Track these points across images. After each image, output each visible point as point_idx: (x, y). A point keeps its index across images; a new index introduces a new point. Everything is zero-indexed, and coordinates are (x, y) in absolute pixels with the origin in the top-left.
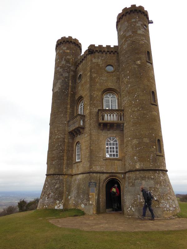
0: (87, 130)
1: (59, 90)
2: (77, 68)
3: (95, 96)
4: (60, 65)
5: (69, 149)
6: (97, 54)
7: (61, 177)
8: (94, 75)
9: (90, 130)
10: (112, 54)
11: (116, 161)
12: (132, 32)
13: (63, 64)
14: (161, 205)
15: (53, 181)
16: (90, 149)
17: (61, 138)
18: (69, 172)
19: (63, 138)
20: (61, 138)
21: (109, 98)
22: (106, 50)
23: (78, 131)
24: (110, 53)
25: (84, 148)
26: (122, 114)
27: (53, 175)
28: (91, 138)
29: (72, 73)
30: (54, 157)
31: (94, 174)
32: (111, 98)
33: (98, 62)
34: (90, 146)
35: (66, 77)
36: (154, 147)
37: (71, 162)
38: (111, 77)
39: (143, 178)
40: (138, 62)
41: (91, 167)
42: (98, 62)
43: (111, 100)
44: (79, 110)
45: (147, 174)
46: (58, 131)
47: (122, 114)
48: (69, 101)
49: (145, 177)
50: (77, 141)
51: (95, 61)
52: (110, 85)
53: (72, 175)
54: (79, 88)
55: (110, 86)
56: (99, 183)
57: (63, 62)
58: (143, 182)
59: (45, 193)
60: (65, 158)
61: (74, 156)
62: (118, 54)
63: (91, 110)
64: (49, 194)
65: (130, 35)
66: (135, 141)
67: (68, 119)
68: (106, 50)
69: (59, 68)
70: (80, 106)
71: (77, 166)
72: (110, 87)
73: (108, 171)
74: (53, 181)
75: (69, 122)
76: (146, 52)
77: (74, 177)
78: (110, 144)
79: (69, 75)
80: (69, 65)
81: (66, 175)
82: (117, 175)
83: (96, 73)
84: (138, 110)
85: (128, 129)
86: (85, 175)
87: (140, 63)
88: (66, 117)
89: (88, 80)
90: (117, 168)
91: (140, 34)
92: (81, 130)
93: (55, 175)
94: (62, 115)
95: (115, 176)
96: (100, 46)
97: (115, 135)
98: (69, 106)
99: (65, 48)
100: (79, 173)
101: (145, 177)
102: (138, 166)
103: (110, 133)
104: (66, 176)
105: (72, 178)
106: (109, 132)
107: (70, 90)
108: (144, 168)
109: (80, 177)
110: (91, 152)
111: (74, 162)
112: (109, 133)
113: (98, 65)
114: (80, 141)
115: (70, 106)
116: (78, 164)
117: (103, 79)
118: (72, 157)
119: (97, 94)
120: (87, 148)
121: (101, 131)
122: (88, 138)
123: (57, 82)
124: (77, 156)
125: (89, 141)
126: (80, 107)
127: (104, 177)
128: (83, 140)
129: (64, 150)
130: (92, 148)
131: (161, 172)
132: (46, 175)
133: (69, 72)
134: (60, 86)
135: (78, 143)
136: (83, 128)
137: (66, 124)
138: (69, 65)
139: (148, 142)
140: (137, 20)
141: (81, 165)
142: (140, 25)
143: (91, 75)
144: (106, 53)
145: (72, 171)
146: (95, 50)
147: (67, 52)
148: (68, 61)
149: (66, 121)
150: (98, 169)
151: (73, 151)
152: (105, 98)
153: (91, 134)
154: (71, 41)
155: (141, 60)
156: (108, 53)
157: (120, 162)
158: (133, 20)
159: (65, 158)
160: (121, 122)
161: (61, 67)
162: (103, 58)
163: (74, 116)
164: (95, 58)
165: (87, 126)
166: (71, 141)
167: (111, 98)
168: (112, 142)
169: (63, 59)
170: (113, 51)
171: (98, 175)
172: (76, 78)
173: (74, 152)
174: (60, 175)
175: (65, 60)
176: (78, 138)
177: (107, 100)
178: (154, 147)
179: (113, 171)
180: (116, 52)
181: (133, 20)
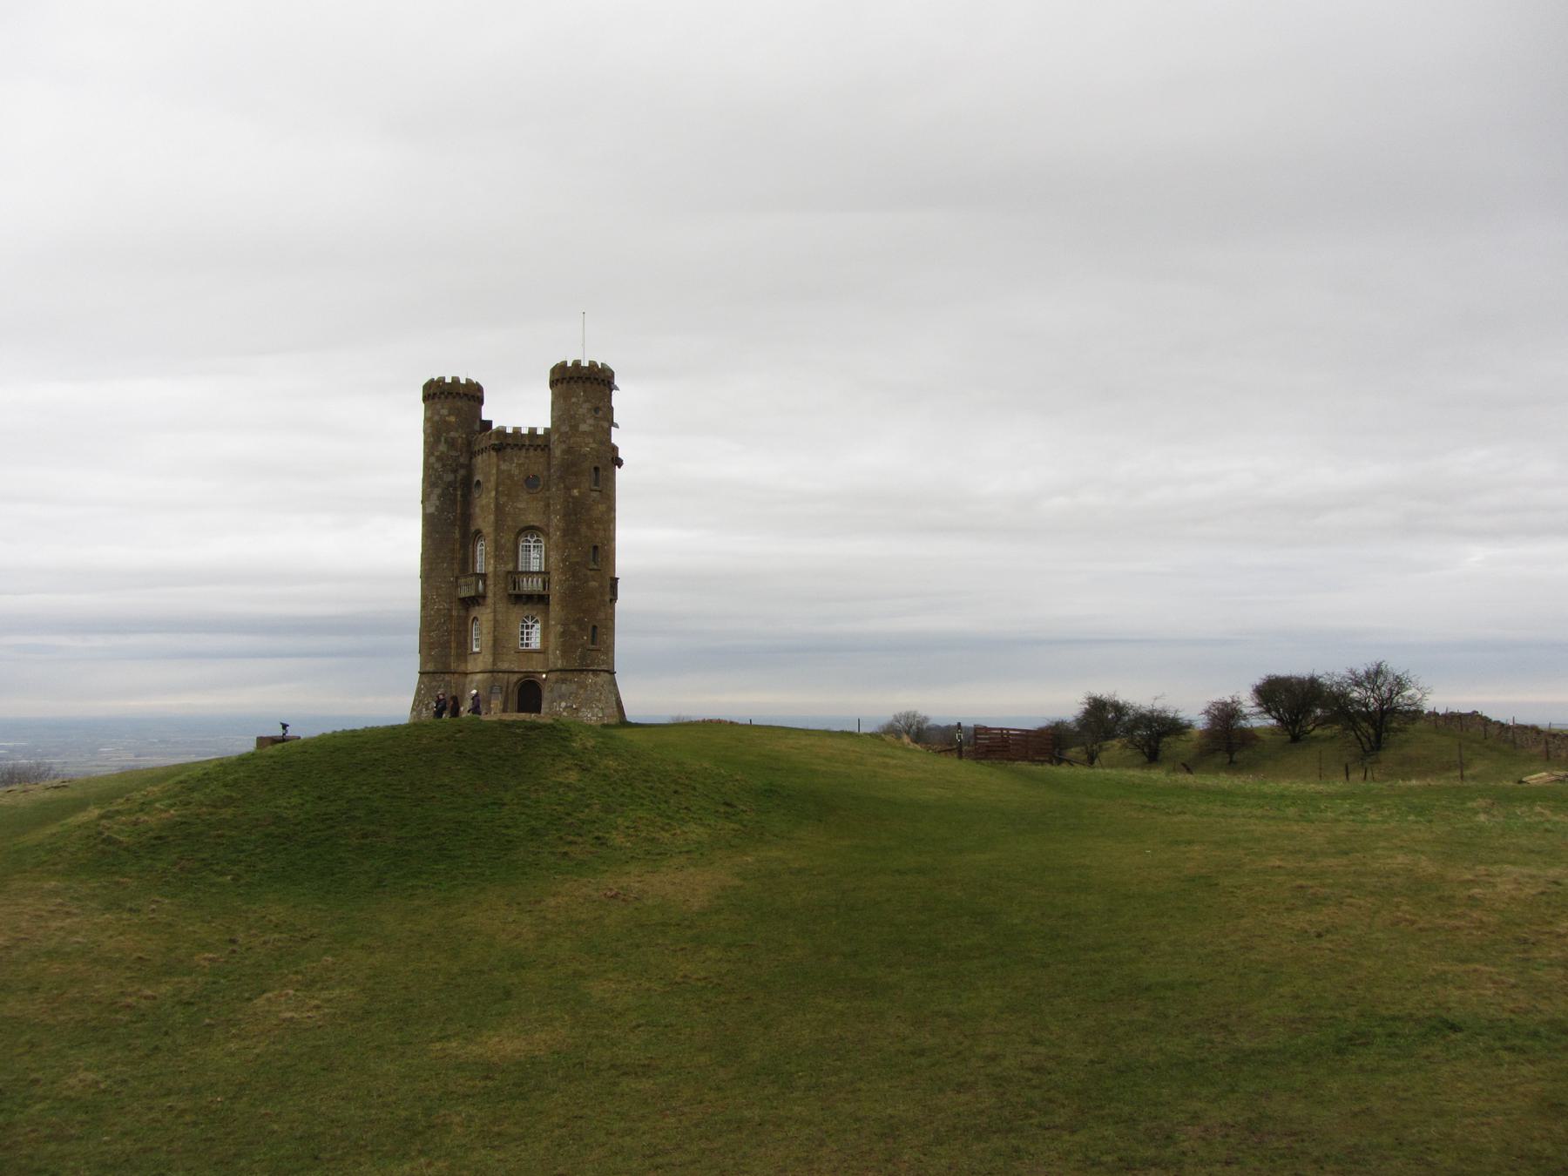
0: (490, 601)
1: (436, 511)
2: (471, 458)
3: (503, 541)
4: (436, 454)
5: (461, 629)
6: (509, 450)
7: (447, 677)
8: (503, 500)
9: (495, 604)
10: (539, 450)
11: (535, 655)
12: (570, 426)
13: (442, 453)
14: (580, 714)
15: (434, 684)
16: (494, 636)
17: (445, 609)
18: (462, 668)
19: (448, 609)
20: (445, 609)
21: (529, 542)
22: (527, 443)
23: (476, 600)
24: (535, 450)
25: (484, 631)
26: (547, 579)
27: (434, 673)
28: (495, 616)
29: (462, 472)
30: (432, 643)
31: (500, 674)
32: (535, 542)
33: (510, 470)
34: (494, 631)
35: (450, 484)
36: (585, 638)
37: (464, 651)
38: (535, 503)
39: (564, 681)
40: (575, 491)
41: (494, 663)
42: (510, 470)
43: (534, 546)
44: (478, 553)
45: (569, 676)
46: (438, 595)
47: (547, 579)
48: (457, 535)
49: (566, 680)
50: (474, 616)
51: (505, 468)
52: (532, 519)
53: (467, 674)
54: (477, 510)
55: (533, 521)
56: (507, 687)
57: (443, 447)
58: (564, 686)
59: (420, 701)
60: (453, 645)
61: (469, 641)
62: (549, 449)
63: (496, 567)
64: (429, 703)
65: (567, 433)
66: (559, 628)
67: (457, 572)
68: (527, 443)
69: (432, 460)
70: (479, 545)
71: (475, 659)
72: (532, 524)
73: (522, 670)
74: (434, 684)
75: (457, 578)
76: (592, 470)
77: (470, 677)
78: (527, 627)
79: (456, 477)
80: (454, 453)
81: (454, 673)
82: (537, 675)
83: (506, 495)
84: (567, 579)
85: (555, 607)
86: (486, 675)
87: (577, 494)
88: (453, 570)
89: (492, 506)
90: (535, 665)
91: (584, 433)
92: (480, 601)
93: (437, 673)
94: (445, 565)
95: (533, 677)
96: (517, 431)
97: (535, 613)
98: (458, 546)
99: (445, 412)
100: (478, 670)
101: (566, 680)
102: (559, 666)
103: (528, 609)
104: (456, 676)
105: (466, 677)
106: (525, 607)
107: (458, 511)
108: (567, 668)
109: (479, 677)
110: (495, 640)
111: (469, 652)
112: (527, 610)
113: (511, 476)
114: (479, 617)
115: (461, 546)
116: (476, 656)
117: (519, 506)
118: (466, 642)
119: (507, 539)
120: (489, 633)
121: (511, 606)
122: (491, 616)
123: (432, 492)
124: (474, 642)
125: (492, 623)
126: (479, 548)
127: (515, 678)
128: (484, 618)
129: (451, 631)
130: (496, 633)
131: (591, 673)
132: (420, 672)
133: (455, 471)
134: (438, 503)
135: (475, 619)
136: (484, 597)
137: (452, 582)
138: (454, 453)
139: (575, 630)
140: (581, 399)
141: (481, 658)
142: (585, 411)
143: (497, 499)
144: (528, 450)
145: (466, 668)
146: (504, 445)
147: (450, 422)
148: (451, 444)
149: (453, 576)
150: (505, 666)
151: (467, 631)
152: (523, 542)
153: (495, 612)
154: (457, 393)
155: (580, 488)
156: (531, 450)
157: (542, 655)
158: (574, 400)
159: (453, 645)
160: (544, 593)
161: (439, 459)
162: (520, 462)
163: (466, 562)
164: (505, 461)
165: (490, 594)
166: (462, 613)
167: (535, 542)
168: (530, 624)
169: (443, 439)
170: (540, 446)
171: (506, 676)
172: (467, 486)
173: (469, 634)
174: (444, 673)
175: (445, 443)
176: (475, 612)
177: (526, 546)
178: (585, 638)
179: (531, 670)
180: (546, 446)
181: (574, 400)
